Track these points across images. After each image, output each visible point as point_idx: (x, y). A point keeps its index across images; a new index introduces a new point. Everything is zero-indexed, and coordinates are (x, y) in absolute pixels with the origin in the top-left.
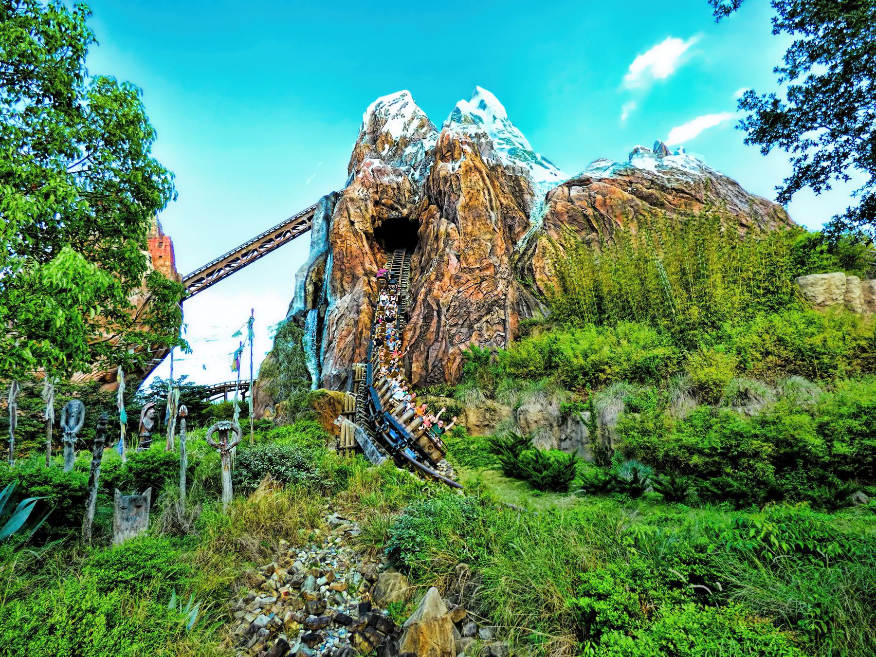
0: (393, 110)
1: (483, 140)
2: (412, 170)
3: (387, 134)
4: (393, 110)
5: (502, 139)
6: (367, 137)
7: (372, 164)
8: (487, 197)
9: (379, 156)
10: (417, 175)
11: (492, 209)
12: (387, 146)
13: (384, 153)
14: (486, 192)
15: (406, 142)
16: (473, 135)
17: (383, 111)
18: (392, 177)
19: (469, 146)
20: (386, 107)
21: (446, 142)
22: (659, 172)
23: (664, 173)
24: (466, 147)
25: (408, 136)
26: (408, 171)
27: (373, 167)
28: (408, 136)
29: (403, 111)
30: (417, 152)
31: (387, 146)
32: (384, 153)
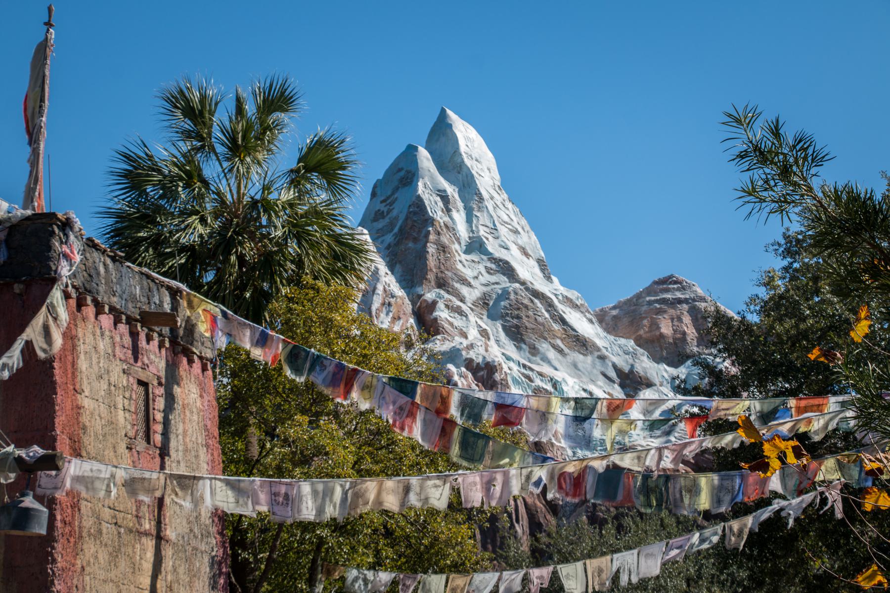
11: (518, 521)
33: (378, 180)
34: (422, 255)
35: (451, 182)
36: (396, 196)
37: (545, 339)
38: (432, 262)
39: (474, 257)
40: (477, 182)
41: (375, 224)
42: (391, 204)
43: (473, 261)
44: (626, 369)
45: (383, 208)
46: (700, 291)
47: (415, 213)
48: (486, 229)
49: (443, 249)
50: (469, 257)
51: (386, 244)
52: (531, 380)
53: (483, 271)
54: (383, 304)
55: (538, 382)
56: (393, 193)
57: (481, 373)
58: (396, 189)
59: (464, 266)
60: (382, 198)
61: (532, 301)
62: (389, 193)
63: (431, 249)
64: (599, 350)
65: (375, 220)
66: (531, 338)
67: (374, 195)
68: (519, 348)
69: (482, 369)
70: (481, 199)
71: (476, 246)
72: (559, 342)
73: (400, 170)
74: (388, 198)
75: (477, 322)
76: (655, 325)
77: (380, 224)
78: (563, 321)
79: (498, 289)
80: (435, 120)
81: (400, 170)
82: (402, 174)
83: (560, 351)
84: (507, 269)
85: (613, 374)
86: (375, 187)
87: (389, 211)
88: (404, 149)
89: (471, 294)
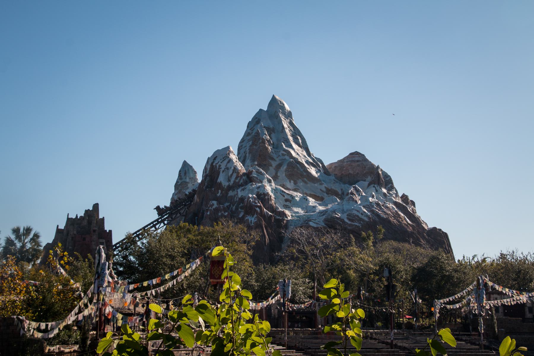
0: (223, 167)
1: (266, 197)
2: (232, 205)
3: (220, 184)
4: (223, 167)
6: (208, 178)
7: (213, 205)
8: (264, 239)
9: (216, 199)
10: (234, 208)
12: (220, 191)
13: (218, 195)
14: (263, 238)
15: (230, 188)
16: (262, 193)
17: (218, 166)
18: (223, 212)
19: (259, 208)
20: (219, 163)
21: (248, 205)
22: (348, 218)
23: (350, 220)
24: (258, 209)
25: (231, 184)
26: (230, 205)
27: (214, 207)
28: (231, 184)
29: (229, 165)
30: (235, 196)
31: (220, 191)
32: (218, 195)
33: (250, 121)
36: (254, 127)
37: (300, 178)
40: (283, 122)
41: (247, 137)
42: (253, 131)
43: (278, 152)
44: (330, 188)
45: (251, 132)
47: (256, 136)
48: (284, 139)
50: (276, 150)
51: (250, 144)
52: (284, 196)
53: (281, 154)
54: (233, 173)
56: (253, 127)
57: (262, 196)
58: (254, 125)
59: (273, 153)
60: (250, 128)
61: (297, 165)
62: (253, 126)
64: (321, 181)
65: (248, 136)
67: (248, 127)
68: (290, 182)
69: (262, 195)
72: (305, 179)
73: (257, 118)
74: (252, 128)
75: (267, 177)
77: (249, 137)
80: (271, 99)
81: (257, 118)
82: (257, 119)
83: (305, 182)
85: (324, 190)
86: (248, 124)
87: (252, 133)
88: (258, 111)
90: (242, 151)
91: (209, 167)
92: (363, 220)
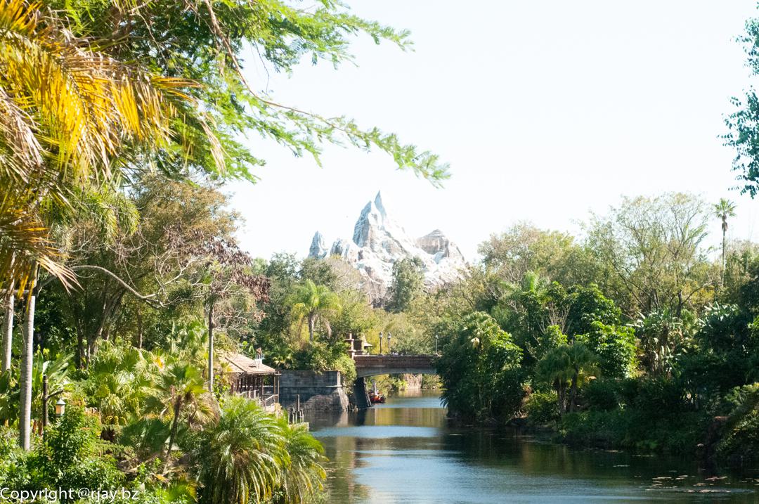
5: (386, 232)
34: (367, 233)
35: (379, 210)
38: (369, 235)
39: (382, 231)
46: (444, 234)
49: (372, 231)
55: (385, 268)
63: (369, 231)
66: (392, 252)
70: (386, 214)
71: (383, 228)
76: (431, 243)
78: (401, 247)
79: (386, 240)
84: (389, 234)
89: (379, 242)
90: (358, 230)
91: (334, 248)
92: (433, 285)
